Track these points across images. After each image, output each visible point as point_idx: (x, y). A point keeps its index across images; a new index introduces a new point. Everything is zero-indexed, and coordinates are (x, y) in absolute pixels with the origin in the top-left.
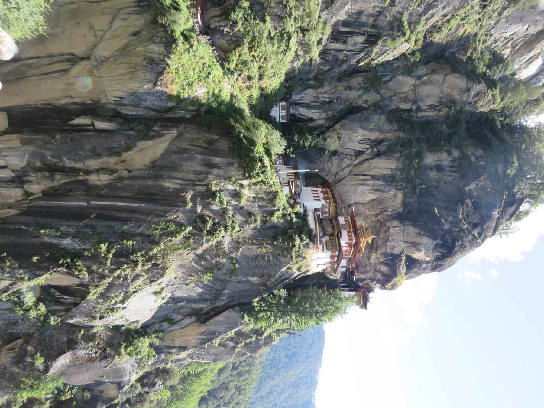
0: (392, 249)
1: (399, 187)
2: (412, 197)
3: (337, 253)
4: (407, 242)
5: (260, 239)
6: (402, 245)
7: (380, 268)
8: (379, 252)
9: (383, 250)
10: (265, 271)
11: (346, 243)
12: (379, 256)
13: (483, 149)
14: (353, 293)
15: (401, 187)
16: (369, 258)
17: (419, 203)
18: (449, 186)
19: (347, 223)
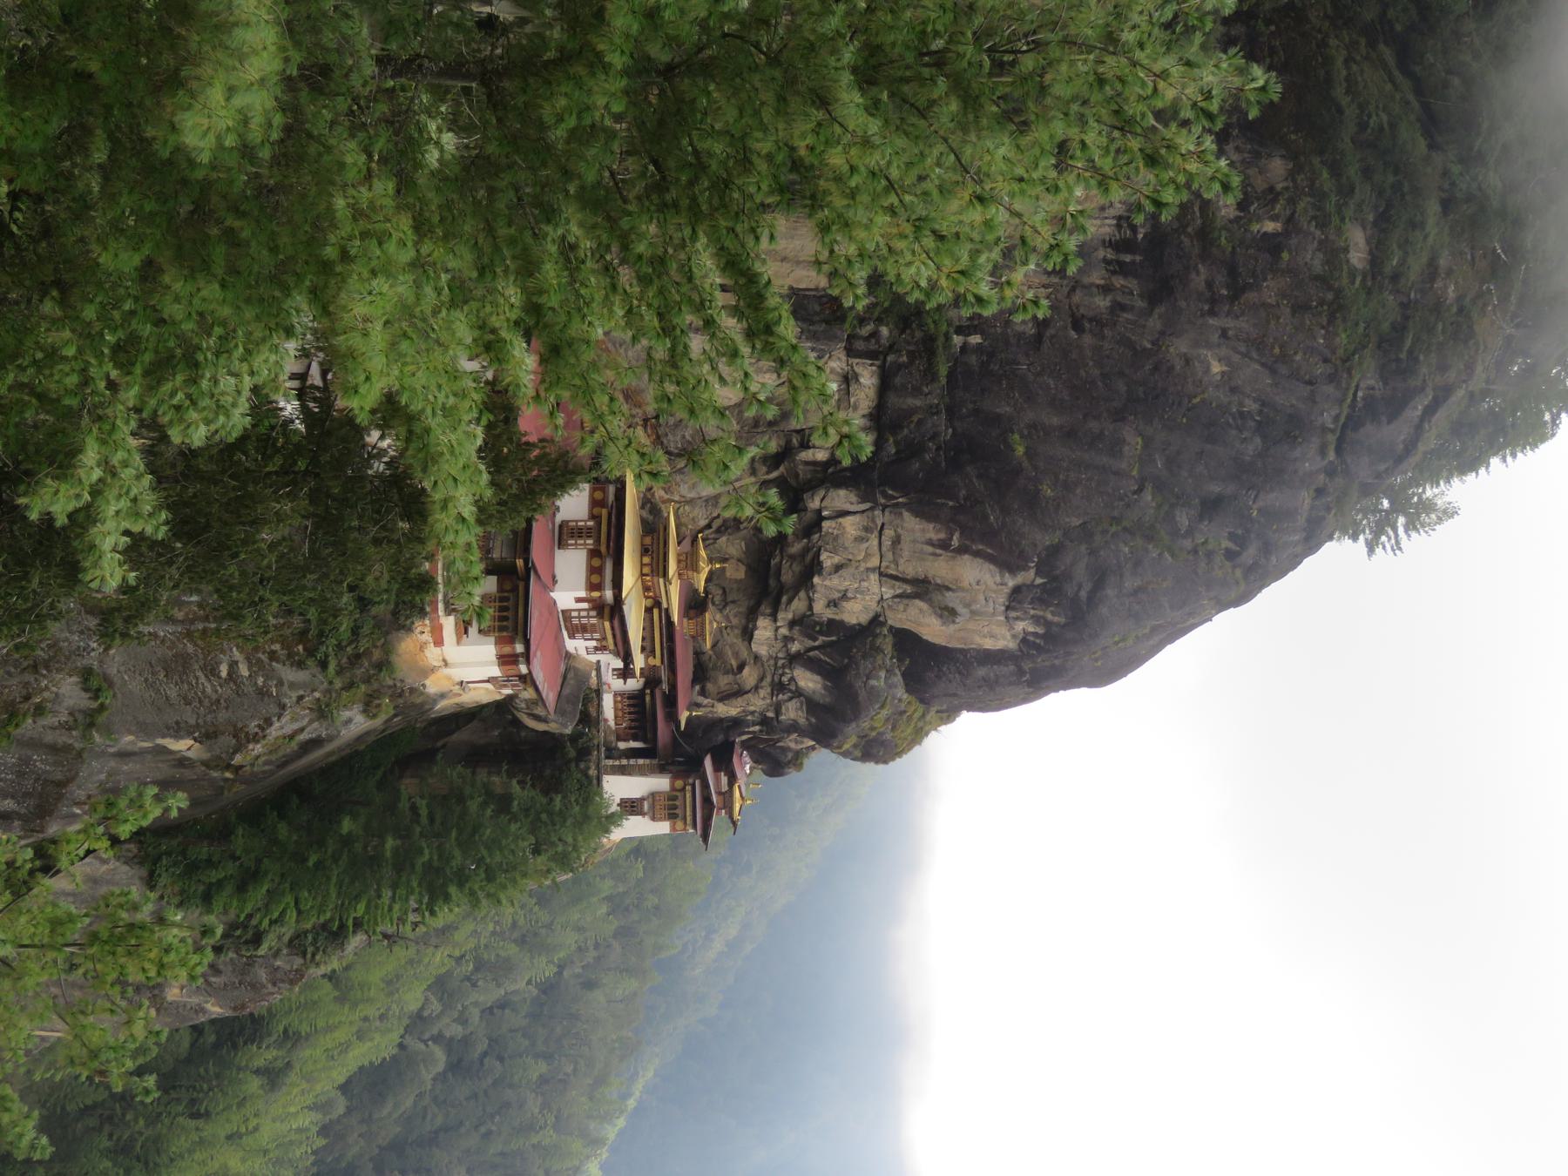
0: (833, 603)
1: (860, 345)
2: (917, 391)
3: (519, 648)
4: (895, 578)
5: (194, 598)
6: (875, 588)
7: (792, 679)
8: (785, 616)
9: (799, 605)
10: (223, 716)
11: (579, 600)
12: (784, 631)
13: (1293, 155)
14: (661, 783)
15: (873, 346)
16: (748, 634)
17: (951, 412)
18: (1088, 339)
19: (596, 511)
